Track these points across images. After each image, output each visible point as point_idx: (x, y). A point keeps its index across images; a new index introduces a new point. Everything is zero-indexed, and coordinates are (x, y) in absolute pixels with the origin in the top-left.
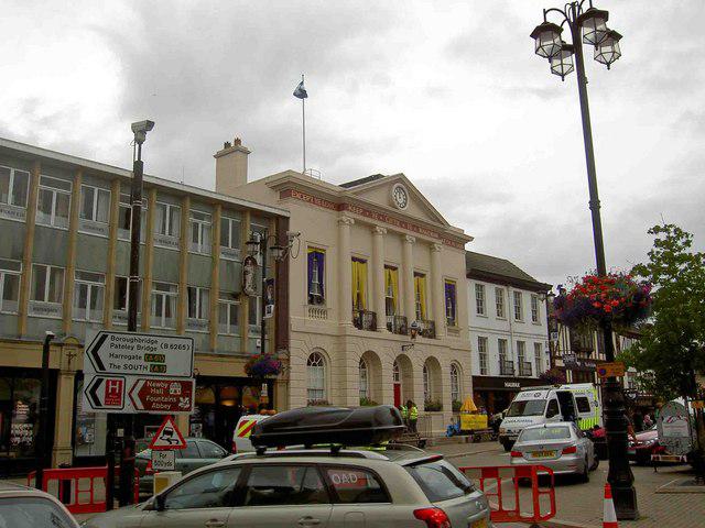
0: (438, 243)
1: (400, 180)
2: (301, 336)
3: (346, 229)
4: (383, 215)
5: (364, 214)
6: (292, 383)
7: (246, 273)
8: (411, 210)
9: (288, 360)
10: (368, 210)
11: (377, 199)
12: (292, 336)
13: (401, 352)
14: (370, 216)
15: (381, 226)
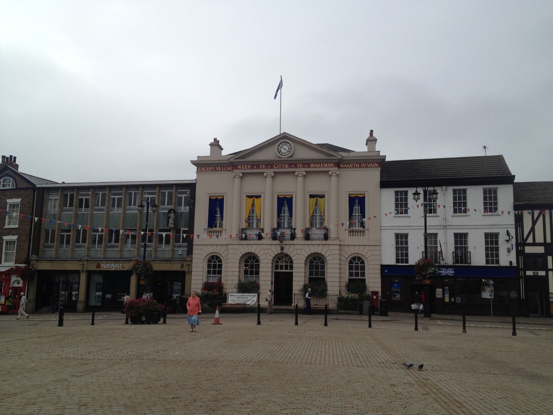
0: (334, 170)
1: (284, 138)
2: (201, 247)
3: (237, 180)
4: (269, 164)
5: (252, 168)
6: (193, 273)
7: (169, 218)
8: (303, 154)
9: (192, 261)
10: (256, 165)
11: (269, 155)
12: (194, 247)
13: (280, 252)
14: (258, 167)
15: (269, 172)
